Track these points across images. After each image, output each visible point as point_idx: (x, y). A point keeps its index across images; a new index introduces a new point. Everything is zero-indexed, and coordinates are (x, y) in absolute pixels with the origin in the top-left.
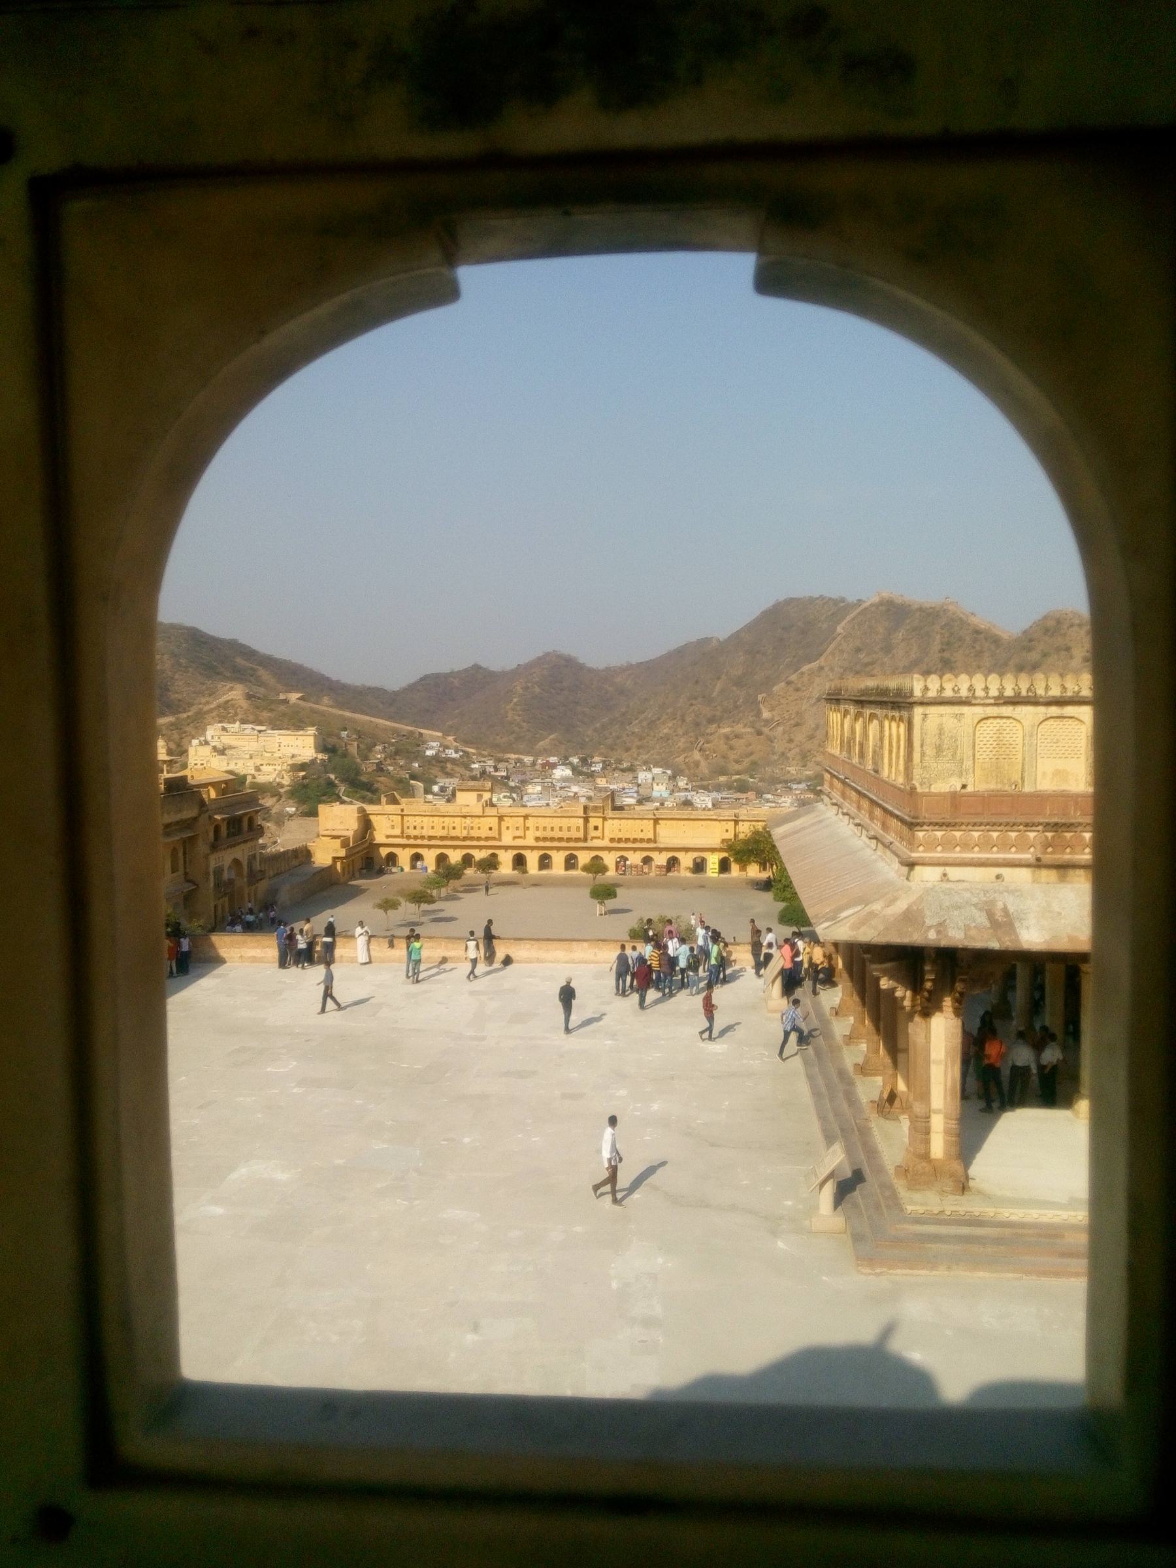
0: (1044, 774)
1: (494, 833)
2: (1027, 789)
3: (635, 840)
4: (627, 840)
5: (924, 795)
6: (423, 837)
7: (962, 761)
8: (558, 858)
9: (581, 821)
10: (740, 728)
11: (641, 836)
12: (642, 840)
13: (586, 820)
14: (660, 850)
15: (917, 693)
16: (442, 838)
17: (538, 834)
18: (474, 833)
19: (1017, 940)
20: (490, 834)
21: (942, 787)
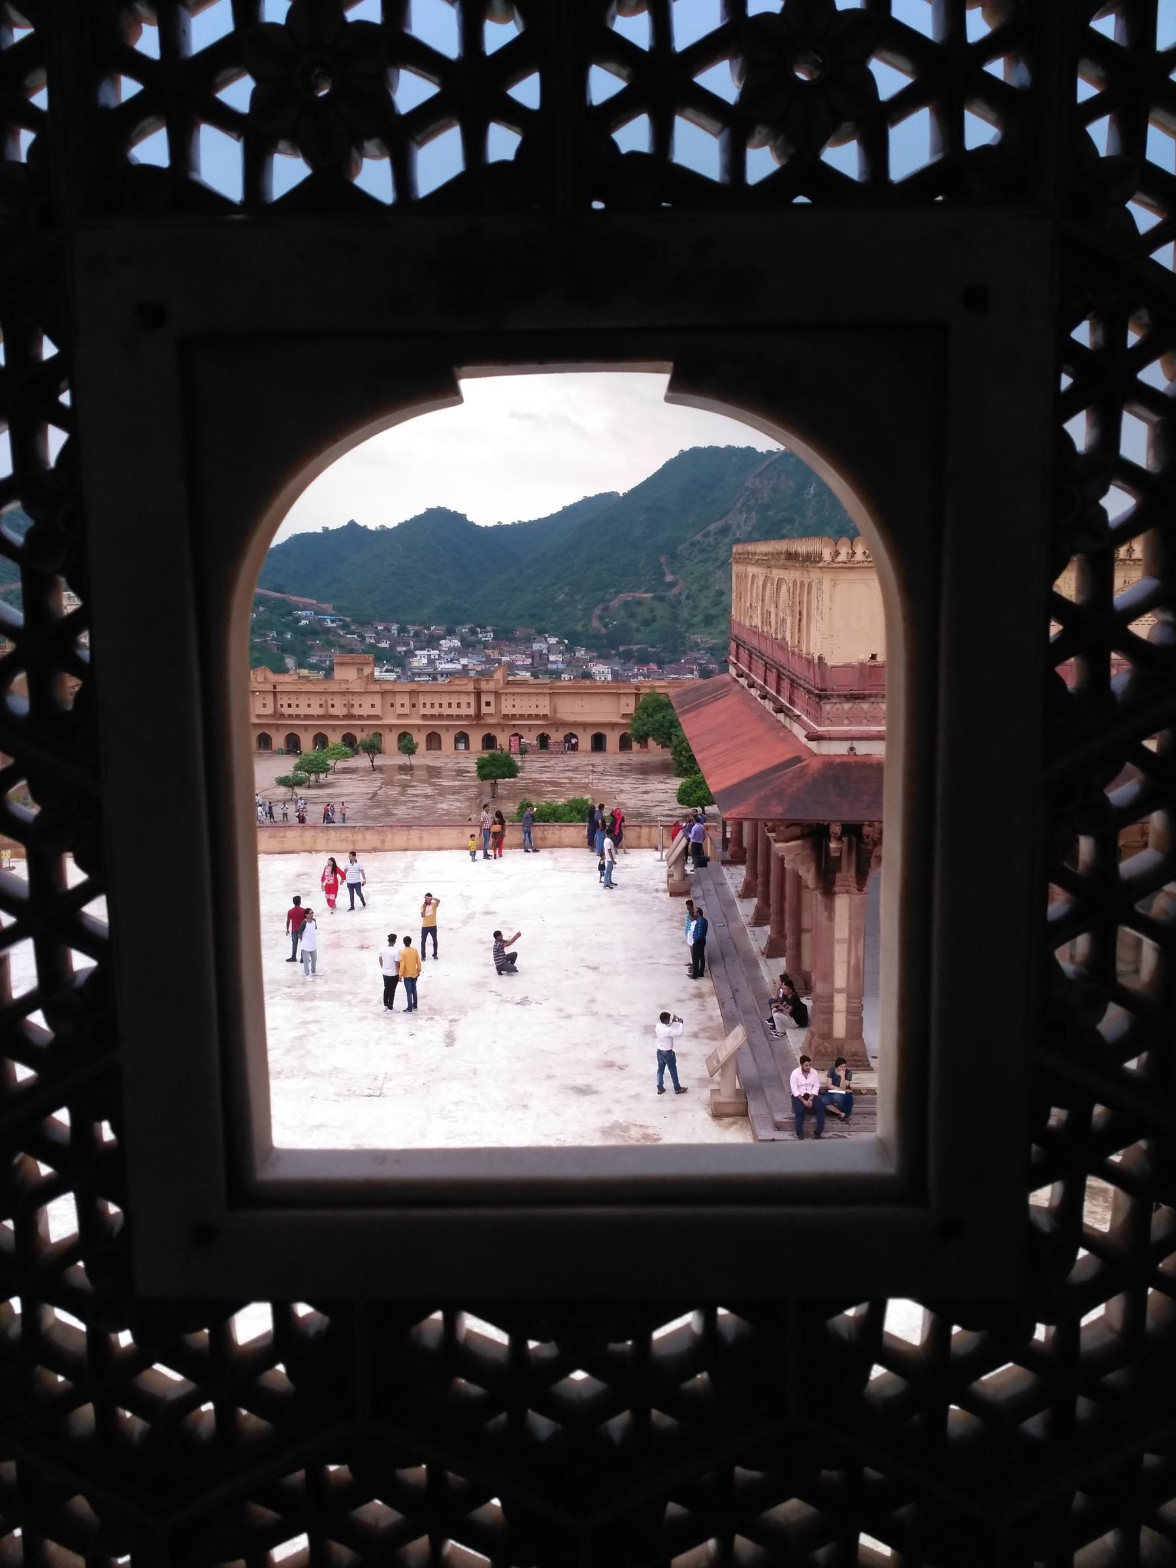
1: (377, 711)
3: (530, 717)
4: (522, 717)
6: (298, 716)
8: (448, 739)
9: (472, 699)
10: (640, 595)
11: (534, 712)
12: (537, 717)
13: (478, 694)
16: (319, 717)
18: (356, 711)
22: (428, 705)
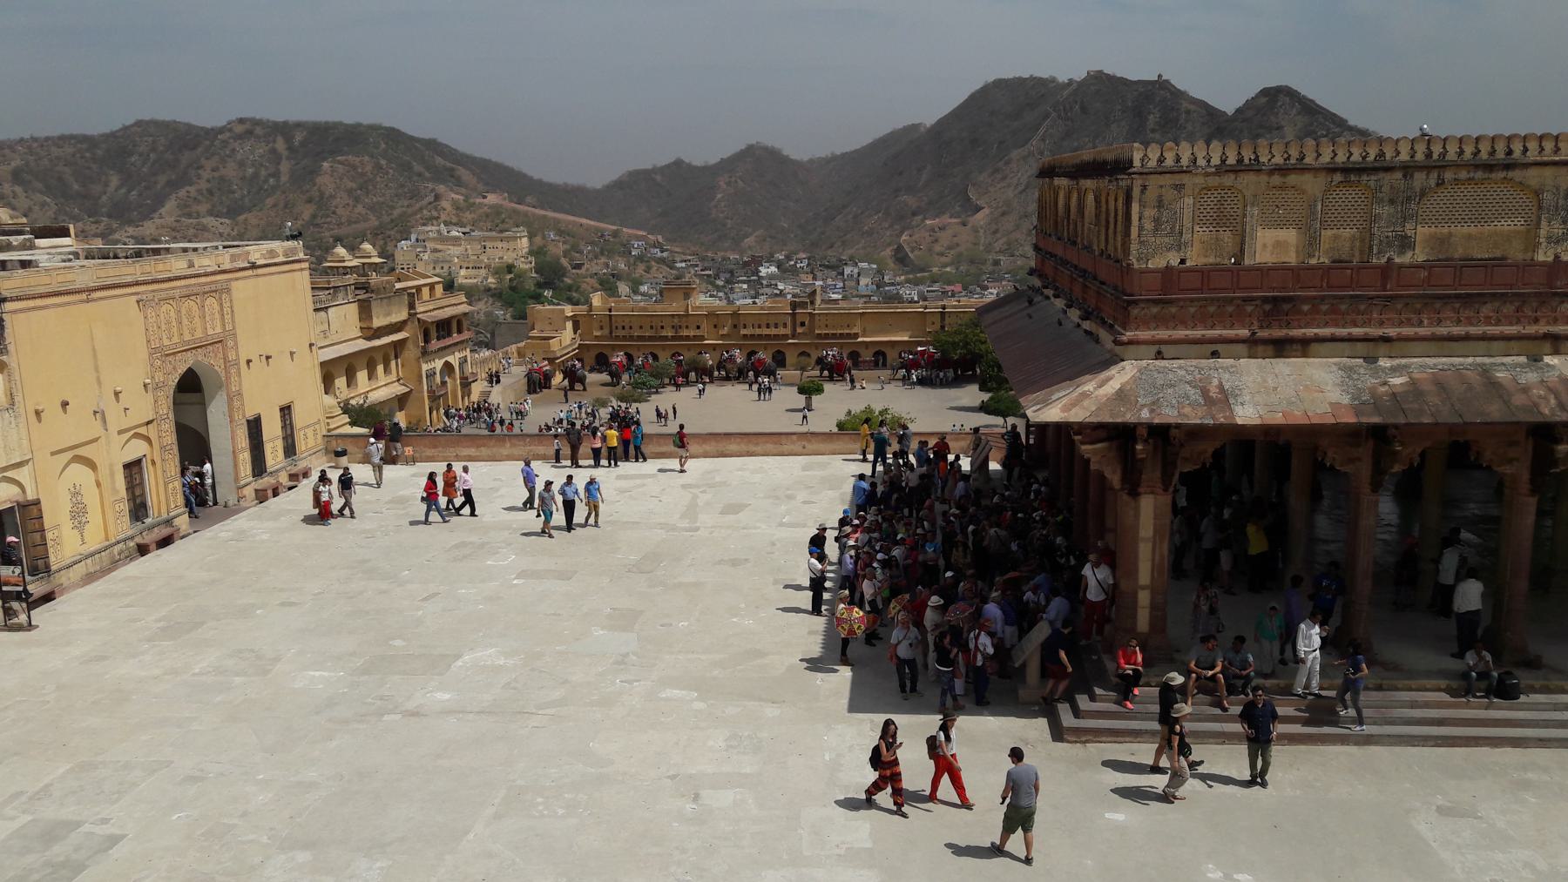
0: (1265, 246)
2: (1247, 262)
5: (1143, 272)
7: (1181, 233)
15: (1137, 163)
19: (1233, 417)
21: (1157, 263)
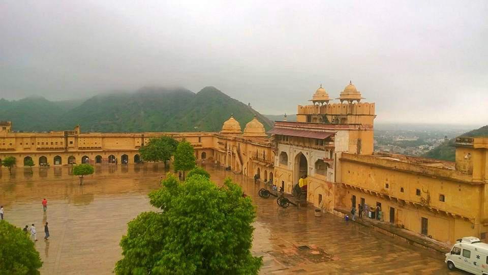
4: (88, 148)
13: (66, 137)
14: (105, 152)
17: (39, 146)
20: (10, 147)
22: (41, 144)
